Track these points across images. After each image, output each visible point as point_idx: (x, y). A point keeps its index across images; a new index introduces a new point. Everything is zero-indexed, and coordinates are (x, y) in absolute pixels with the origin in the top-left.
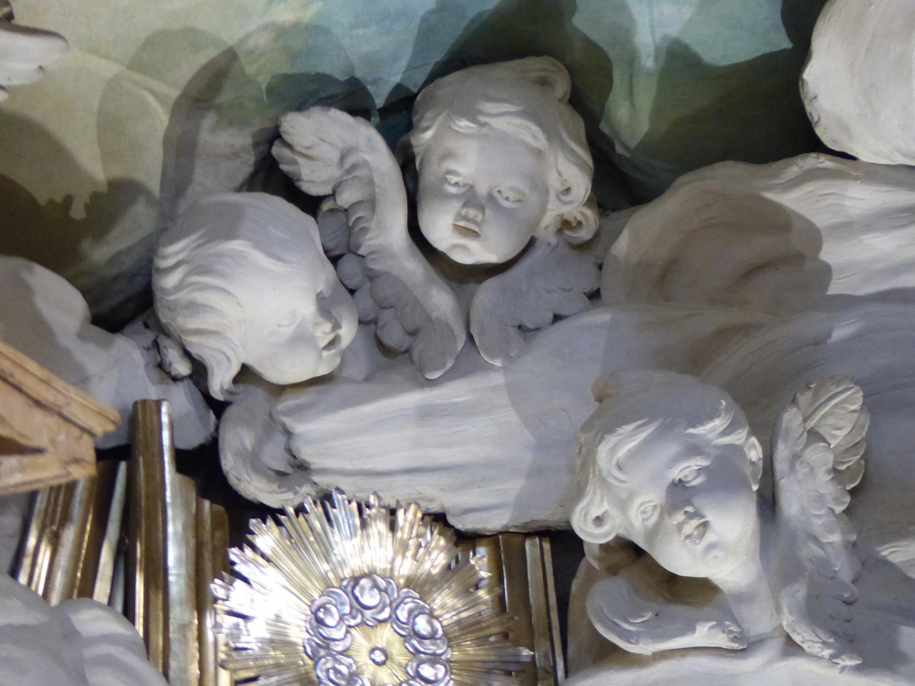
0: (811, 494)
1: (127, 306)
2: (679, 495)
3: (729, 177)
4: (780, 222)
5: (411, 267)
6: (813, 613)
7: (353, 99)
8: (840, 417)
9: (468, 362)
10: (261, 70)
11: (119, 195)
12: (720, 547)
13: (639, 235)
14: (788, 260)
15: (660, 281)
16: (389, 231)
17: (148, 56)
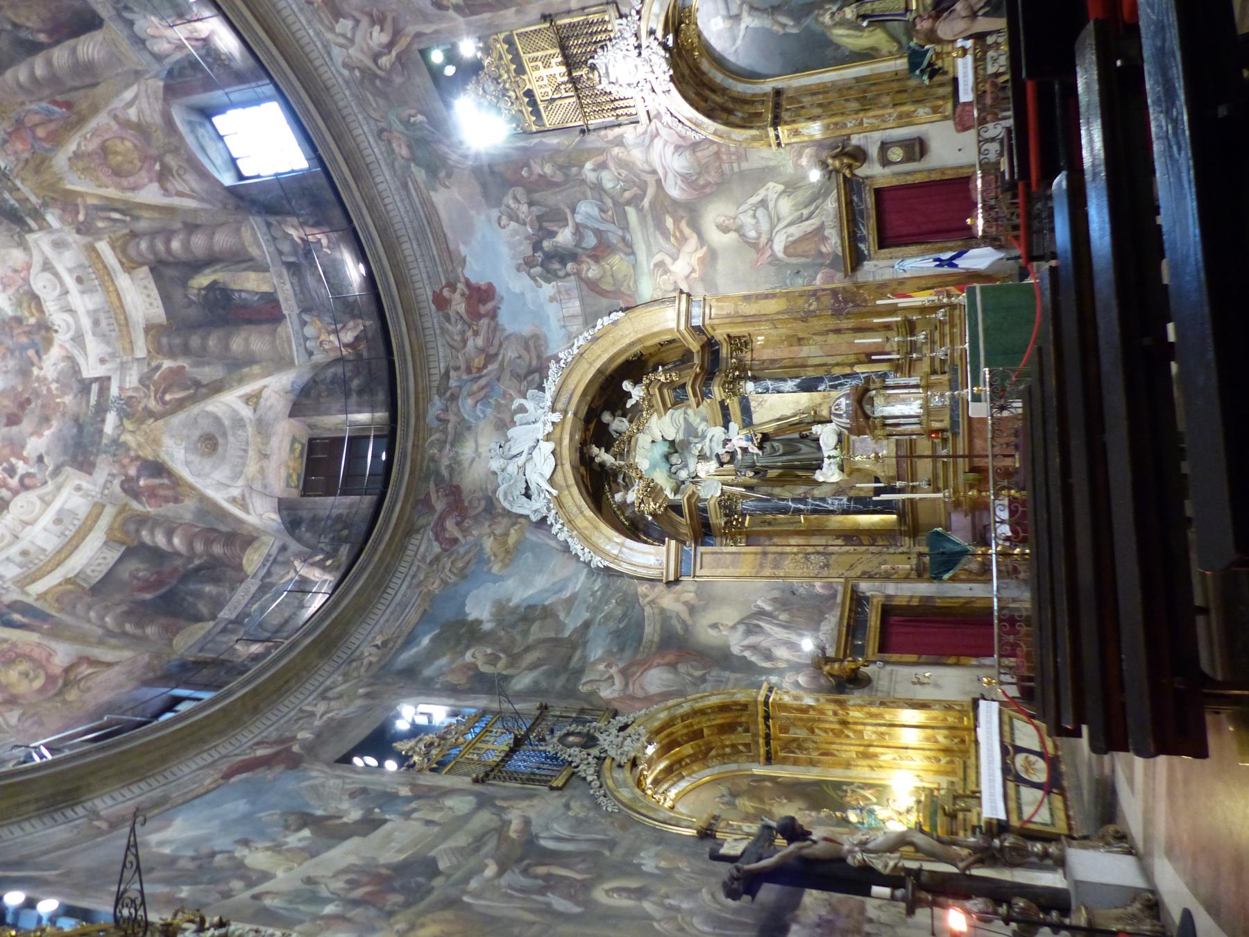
1: (683, 482)
12: (699, 446)
14: (682, 441)
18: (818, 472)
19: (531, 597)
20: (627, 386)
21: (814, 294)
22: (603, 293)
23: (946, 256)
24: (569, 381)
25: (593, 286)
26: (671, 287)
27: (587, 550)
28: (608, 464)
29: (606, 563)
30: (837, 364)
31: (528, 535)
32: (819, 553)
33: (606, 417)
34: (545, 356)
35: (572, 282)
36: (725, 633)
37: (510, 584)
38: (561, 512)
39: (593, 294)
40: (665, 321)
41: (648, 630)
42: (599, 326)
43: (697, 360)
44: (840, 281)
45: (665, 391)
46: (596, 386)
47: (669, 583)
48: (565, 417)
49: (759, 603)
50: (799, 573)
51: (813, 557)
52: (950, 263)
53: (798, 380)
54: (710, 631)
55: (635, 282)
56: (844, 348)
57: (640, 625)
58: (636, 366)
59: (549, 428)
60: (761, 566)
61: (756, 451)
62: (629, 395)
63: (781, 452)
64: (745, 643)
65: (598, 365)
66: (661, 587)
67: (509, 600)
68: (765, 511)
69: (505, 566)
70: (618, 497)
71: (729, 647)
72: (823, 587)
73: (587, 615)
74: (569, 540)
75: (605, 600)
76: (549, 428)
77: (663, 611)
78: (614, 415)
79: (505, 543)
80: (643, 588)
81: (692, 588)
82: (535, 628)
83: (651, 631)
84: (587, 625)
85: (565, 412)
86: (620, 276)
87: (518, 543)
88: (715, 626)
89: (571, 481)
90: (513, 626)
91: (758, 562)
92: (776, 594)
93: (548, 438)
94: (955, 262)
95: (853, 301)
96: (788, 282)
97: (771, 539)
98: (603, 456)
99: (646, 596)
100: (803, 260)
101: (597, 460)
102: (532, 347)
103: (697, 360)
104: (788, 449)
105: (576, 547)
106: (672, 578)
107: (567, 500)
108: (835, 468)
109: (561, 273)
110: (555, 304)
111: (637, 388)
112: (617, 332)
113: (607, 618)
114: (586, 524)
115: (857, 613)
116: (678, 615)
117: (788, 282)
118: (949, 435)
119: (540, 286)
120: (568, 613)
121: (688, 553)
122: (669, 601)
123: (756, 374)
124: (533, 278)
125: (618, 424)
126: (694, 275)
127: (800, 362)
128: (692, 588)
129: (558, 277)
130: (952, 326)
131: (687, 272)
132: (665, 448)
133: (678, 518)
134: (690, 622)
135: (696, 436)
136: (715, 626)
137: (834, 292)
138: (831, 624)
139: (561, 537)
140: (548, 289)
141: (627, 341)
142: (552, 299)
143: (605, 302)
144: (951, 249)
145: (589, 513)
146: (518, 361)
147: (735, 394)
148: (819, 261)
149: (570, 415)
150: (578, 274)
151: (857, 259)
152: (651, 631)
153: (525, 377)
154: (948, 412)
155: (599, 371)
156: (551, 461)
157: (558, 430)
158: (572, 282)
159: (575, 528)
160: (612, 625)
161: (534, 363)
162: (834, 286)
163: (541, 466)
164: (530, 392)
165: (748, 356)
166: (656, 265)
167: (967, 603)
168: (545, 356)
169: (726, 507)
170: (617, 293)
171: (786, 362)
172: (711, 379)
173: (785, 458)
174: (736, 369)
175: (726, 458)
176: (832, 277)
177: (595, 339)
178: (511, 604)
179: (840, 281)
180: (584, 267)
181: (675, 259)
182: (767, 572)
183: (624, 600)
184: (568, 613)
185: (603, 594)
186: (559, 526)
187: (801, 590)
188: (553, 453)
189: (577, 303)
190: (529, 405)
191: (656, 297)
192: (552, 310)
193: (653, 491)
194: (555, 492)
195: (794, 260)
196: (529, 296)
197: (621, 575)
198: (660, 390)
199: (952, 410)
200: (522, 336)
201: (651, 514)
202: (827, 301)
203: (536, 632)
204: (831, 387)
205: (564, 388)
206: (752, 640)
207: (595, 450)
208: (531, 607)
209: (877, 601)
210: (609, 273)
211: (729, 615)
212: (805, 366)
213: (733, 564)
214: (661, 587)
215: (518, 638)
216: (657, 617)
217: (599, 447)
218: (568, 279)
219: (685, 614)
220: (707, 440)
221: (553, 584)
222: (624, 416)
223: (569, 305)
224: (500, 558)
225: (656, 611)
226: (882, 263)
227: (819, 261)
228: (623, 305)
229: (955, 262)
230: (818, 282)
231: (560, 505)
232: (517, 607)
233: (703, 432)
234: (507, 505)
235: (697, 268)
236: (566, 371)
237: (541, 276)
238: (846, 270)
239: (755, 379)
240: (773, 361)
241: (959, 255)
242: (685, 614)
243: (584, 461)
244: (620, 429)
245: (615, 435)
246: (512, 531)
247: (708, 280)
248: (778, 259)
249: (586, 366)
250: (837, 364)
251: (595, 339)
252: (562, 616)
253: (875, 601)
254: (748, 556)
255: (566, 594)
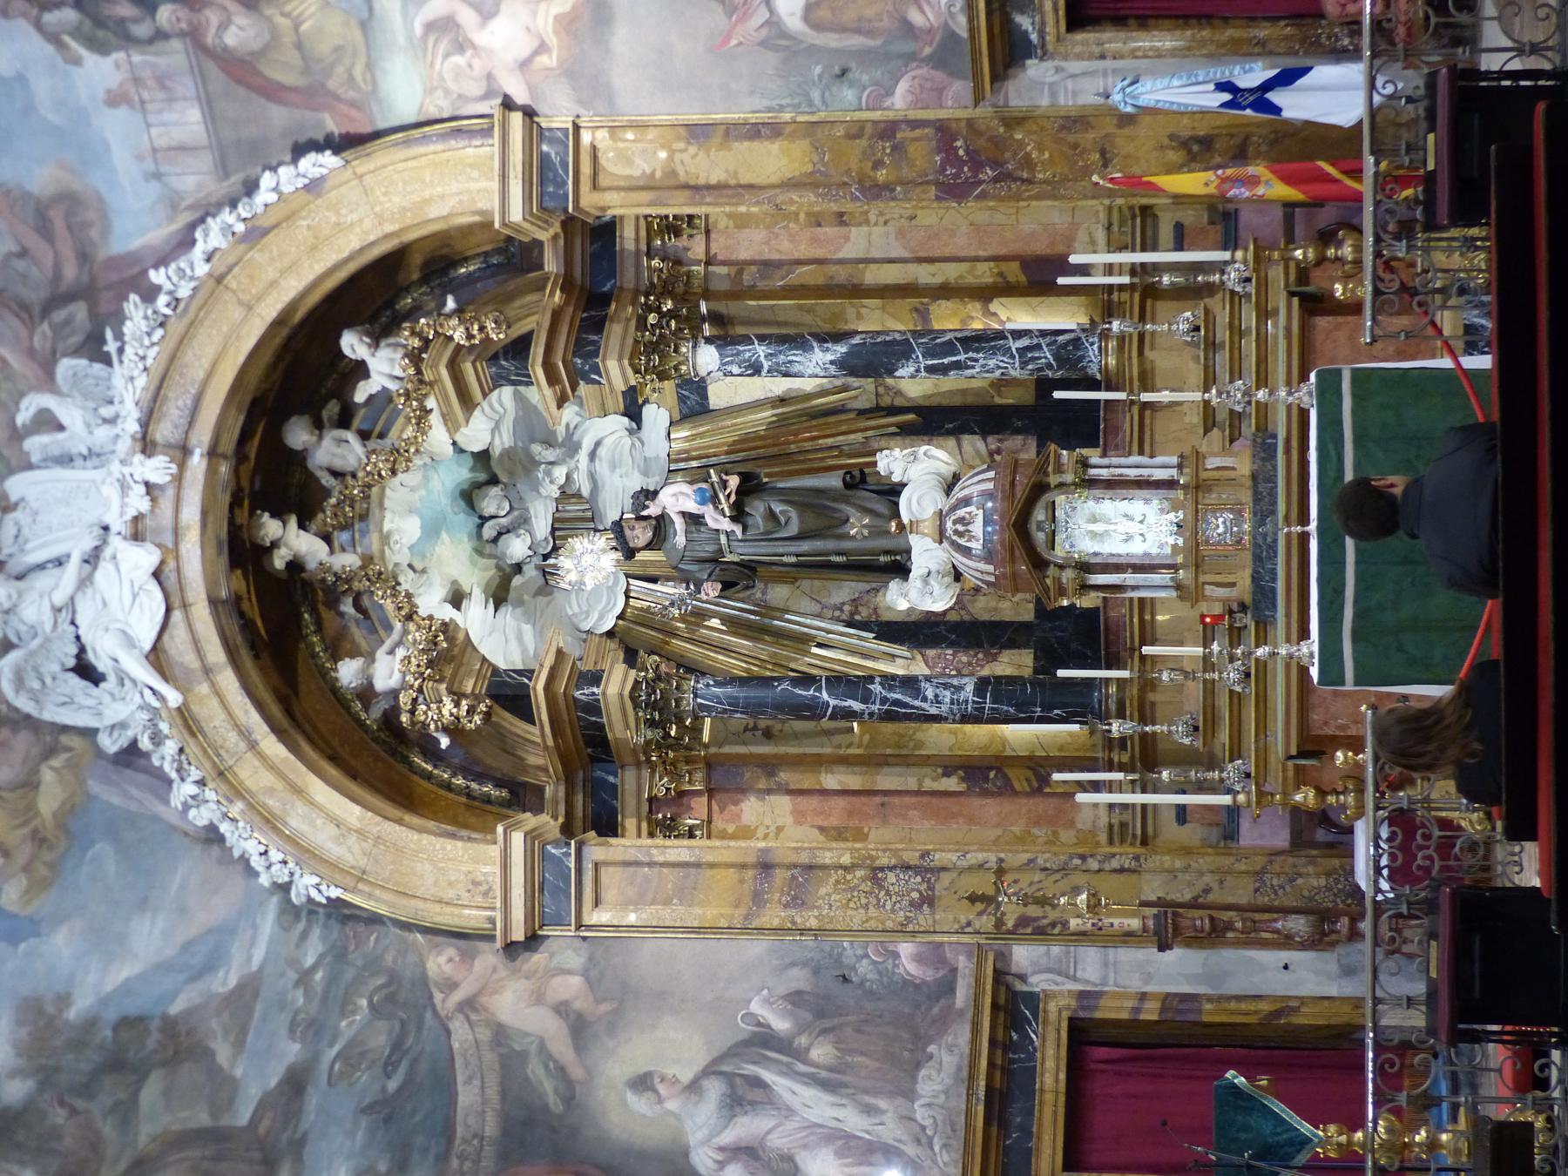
0: (550, 455)
1: (518, 568)
2: (552, 482)
3: (493, 463)
4: (501, 455)
5: (510, 517)
6: (572, 457)
7: (480, 526)
8: (536, 448)
9: (527, 510)
10: (475, 543)
11: (498, 567)
12: (560, 473)
13: (503, 478)
14: (508, 454)
15: (511, 473)
16: (503, 521)
17: (474, 564)
18: (894, 585)
19: (126, 988)
20: (352, 344)
21: (888, 130)
22: (273, 92)
23: (1252, 75)
24: (189, 356)
25: (242, 71)
26: (476, 89)
27: (275, 856)
28: (311, 565)
29: (335, 893)
30: (945, 291)
31: (95, 787)
32: (906, 867)
33: (298, 435)
34: (102, 255)
35: (175, 56)
36: (672, 1105)
37: (61, 945)
38: (192, 749)
39: (242, 92)
40: (462, 189)
41: (467, 1097)
42: (264, 196)
43: (552, 264)
44: (956, 101)
45: (468, 368)
46: (268, 355)
47: (511, 949)
48: (182, 466)
49: (756, 1007)
50: (857, 919)
51: (891, 877)
52: (1259, 99)
53: (841, 349)
54: (631, 1097)
55: (370, 66)
56: (961, 243)
57: (445, 1086)
58: (380, 290)
59: (139, 502)
60: (758, 899)
61: (726, 524)
62: (360, 370)
63: (794, 528)
64: (728, 1137)
65: (270, 310)
66: (488, 958)
67: (64, 1000)
68: (754, 709)
69: (37, 886)
70: (348, 672)
71: (686, 1154)
72: (919, 959)
73: (293, 1051)
74: (224, 828)
75: (337, 999)
76: (139, 502)
77: (500, 1033)
78: (318, 425)
79: (31, 810)
80: (440, 962)
81: (575, 960)
82: (151, 1092)
83: (475, 1101)
84: (295, 1083)
85: (182, 452)
86: (324, 48)
87: (69, 811)
88: (643, 1083)
89: (216, 653)
90: (87, 1089)
91: (748, 887)
92: (799, 979)
93: (137, 532)
94: (1275, 97)
95: (996, 163)
96: (816, 95)
97: (771, 774)
98: (294, 542)
99: (451, 986)
100: (856, 41)
101: (279, 561)
102: (59, 224)
103: (552, 264)
104: (813, 522)
105: (245, 841)
106: (518, 935)
107: (209, 713)
108: (929, 543)
109: (142, 30)
110: (122, 112)
111: (384, 353)
112: (320, 214)
113: (352, 1056)
114: (268, 778)
115: (1008, 1047)
116: (542, 1048)
117: (816, 95)
118: (1248, 620)
119: (77, 61)
120: (239, 1045)
121: (559, 863)
122: (516, 1003)
123: (721, 307)
124: (54, 38)
125: (332, 450)
126: (543, 60)
127: (841, 274)
128: (575, 960)
129: (129, 41)
130: (1264, 313)
131: (523, 48)
132: (463, 473)
133: (519, 726)
134: (576, 1072)
135: (549, 442)
136: (643, 1083)
137: (944, 133)
138: (945, 1074)
139: (200, 817)
140: (101, 71)
141: (355, 244)
142: (115, 99)
143: (278, 116)
144: (1261, 50)
145: (273, 747)
146: (21, 265)
147: (663, 376)
148: (907, 47)
149: (197, 461)
150: (194, 36)
151: (1009, 51)
152: (475, 1101)
153: (46, 311)
154: (1247, 557)
155: (278, 323)
156: (154, 601)
157: (166, 504)
158: (175, 56)
159: (236, 791)
160: (366, 1081)
161: (70, 272)
162: (942, 114)
163: (125, 608)
164: (67, 367)
165: (697, 249)
166: (430, 27)
167: (1277, 1014)
168: (102, 255)
169: (653, 706)
170: (314, 94)
171: (802, 275)
172: (597, 325)
173: (805, 546)
174: (666, 290)
175: (640, 535)
176: (940, 91)
177: (255, 234)
178: (72, 1014)
179: (956, 101)
180: (212, 17)
181: (487, 14)
182: (774, 916)
183: (391, 999)
184: (239, 1045)
185: (331, 981)
186: (189, 789)
187: (864, 968)
188: (157, 575)
189: (194, 115)
190: (68, 412)
191: (434, 113)
192: (116, 127)
193: (446, 653)
194: (174, 698)
195: (831, 40)
196: (42, 87)
197: (374, 920)
198: (454, 367)
199: (1257, 558)
200: (27, 196)
201: (445, 730)
202: (922, 154)
203: (159, 1110)
204: (931, 370)
205: (175, 376)
206: (746, 1127)
207: (271, 527)
208: (131, 1024)
209: (1057, 1012)
210: (288, 40)
211: (677, 1046)
212: (857, 291)
213: (684, 895)
214: (488, 958)
215: (108, 1130)
216: (490, 1057)
217: (278, 514)
218: (161, 46)
219: (562, 1048)
220: (583, 457)
221: (187, 947)
222: (344, 421)
223: (168, 117)
224: (21, 859)
225: (484, 1035)
226: (1075, 66)
227: (907, 47)
228: (332, 126)
229: (1275, 97)
230: (900, 100)
231: (186, 719)
232: (91, 1024)
233: (570, 434)
234: (24, 704)
235: (553, 41)
236: (176, 327)
237: (76, 33)
238: (976, 76)
239: (722, 341)
240: (767, 266)
241: (1287, 78)
242: (562, 1048)
243: (242, 552)
244: (338, 464)
245: (327, 480)
246: (47, 775)
247: (585, 76)
248: (785, 34)
249: (237, 313)
250: (945, 291)
251: (255, 234)
252: (223, 1054)
253: (1052, 1007)
254: (721, 874)
255: (226, 980)
